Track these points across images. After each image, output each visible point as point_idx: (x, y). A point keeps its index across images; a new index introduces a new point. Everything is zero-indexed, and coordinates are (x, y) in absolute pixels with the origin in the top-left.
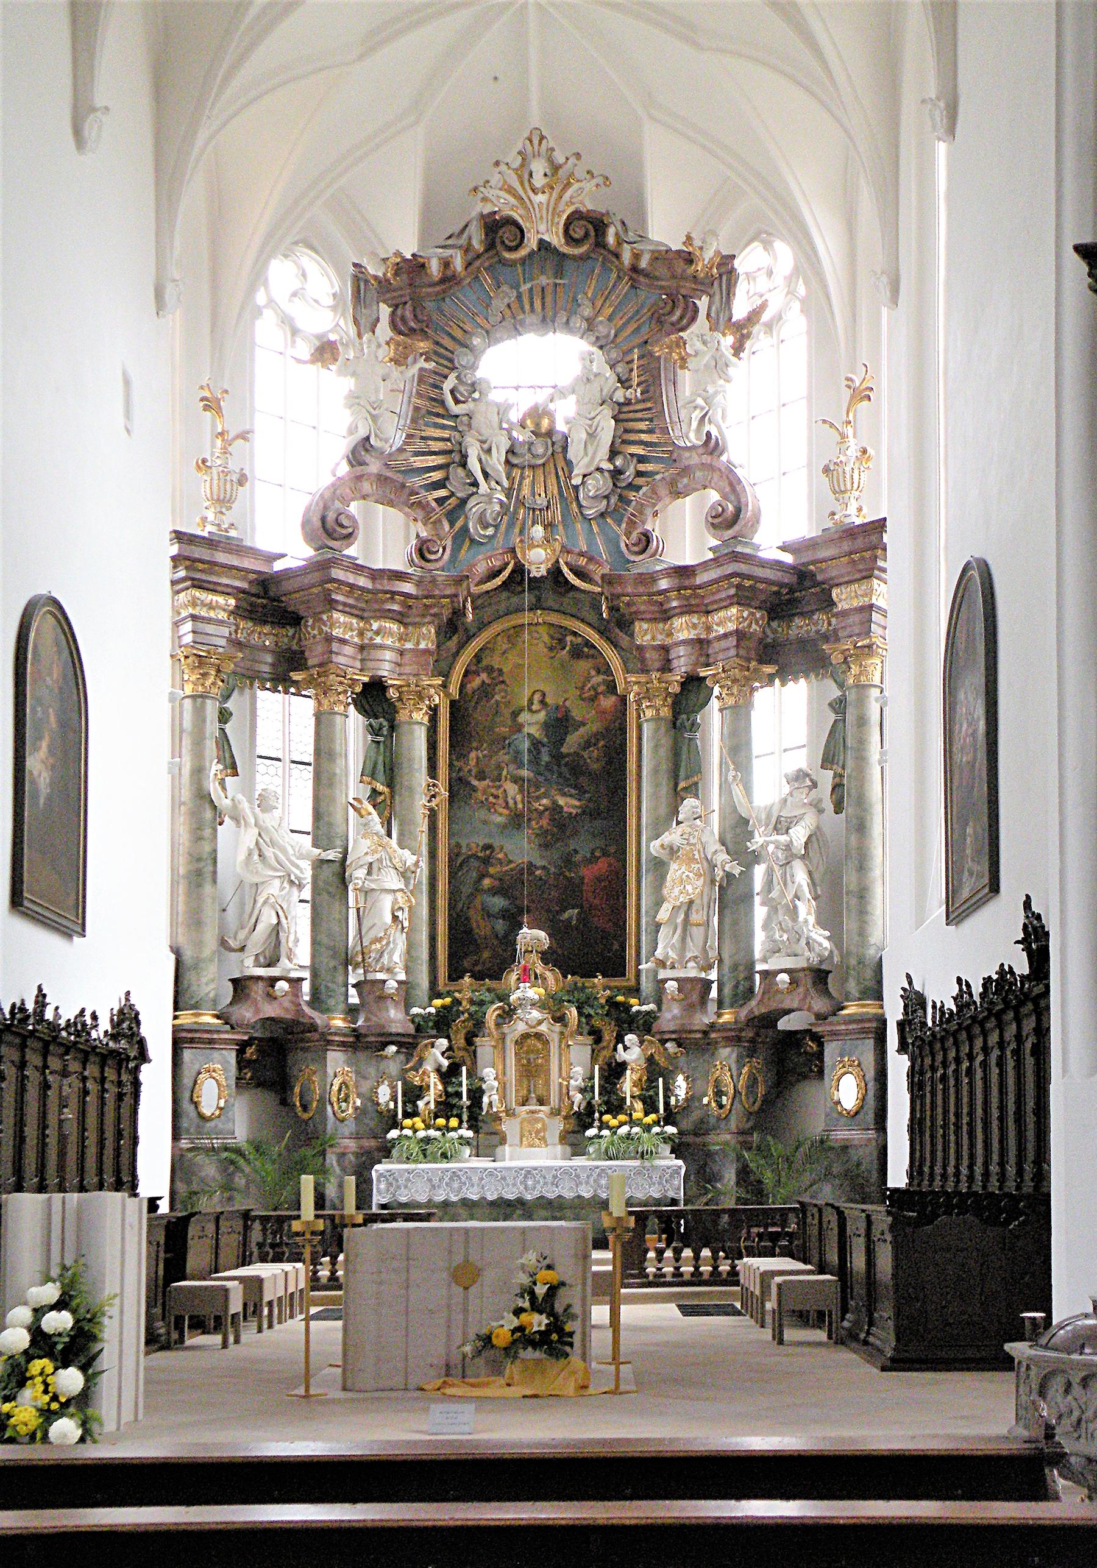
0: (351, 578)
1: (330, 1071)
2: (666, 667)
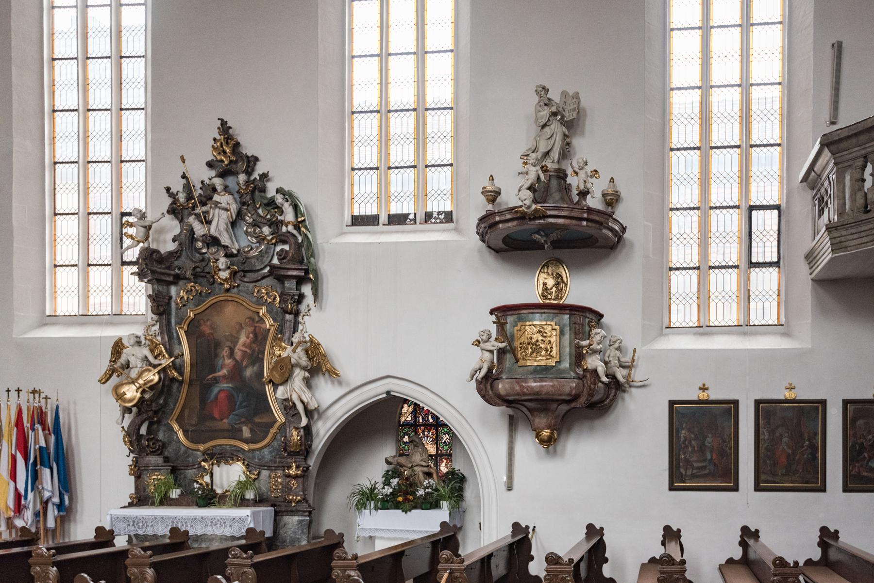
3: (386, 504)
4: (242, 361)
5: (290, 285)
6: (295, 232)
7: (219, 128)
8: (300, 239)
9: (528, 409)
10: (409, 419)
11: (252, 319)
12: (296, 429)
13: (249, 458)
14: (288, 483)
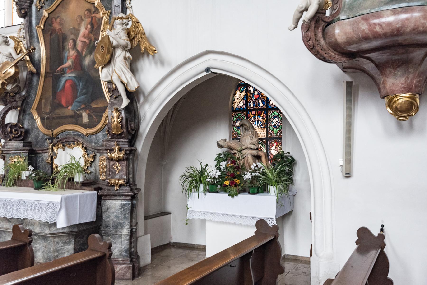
3: (215, 187)
4: (82, 51)
9: (377, 65)
10: (241, 104)
11: (89, 10)
12: (117, 110)
13: (87, 141)
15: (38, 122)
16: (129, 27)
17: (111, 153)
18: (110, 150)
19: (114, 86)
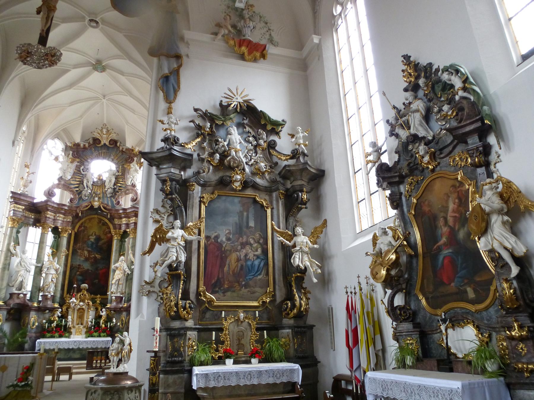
0: (52, 205)
1: (31, 316)
2: (120, 229)
4: (455, 225)
5: (474, 141)
6: (465, 94)
7: (403, 61)
8: (472, 98)
11: (454, 186)
12: (507, 281)
14: (515, 348)
15: (424, 302)
16: (499, 190)
17: (510, 332)
18: (508, 328)
19: (497, 254)
